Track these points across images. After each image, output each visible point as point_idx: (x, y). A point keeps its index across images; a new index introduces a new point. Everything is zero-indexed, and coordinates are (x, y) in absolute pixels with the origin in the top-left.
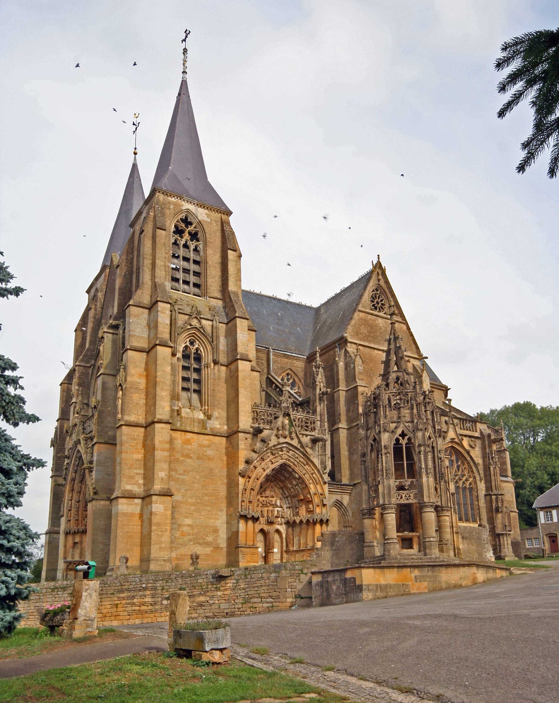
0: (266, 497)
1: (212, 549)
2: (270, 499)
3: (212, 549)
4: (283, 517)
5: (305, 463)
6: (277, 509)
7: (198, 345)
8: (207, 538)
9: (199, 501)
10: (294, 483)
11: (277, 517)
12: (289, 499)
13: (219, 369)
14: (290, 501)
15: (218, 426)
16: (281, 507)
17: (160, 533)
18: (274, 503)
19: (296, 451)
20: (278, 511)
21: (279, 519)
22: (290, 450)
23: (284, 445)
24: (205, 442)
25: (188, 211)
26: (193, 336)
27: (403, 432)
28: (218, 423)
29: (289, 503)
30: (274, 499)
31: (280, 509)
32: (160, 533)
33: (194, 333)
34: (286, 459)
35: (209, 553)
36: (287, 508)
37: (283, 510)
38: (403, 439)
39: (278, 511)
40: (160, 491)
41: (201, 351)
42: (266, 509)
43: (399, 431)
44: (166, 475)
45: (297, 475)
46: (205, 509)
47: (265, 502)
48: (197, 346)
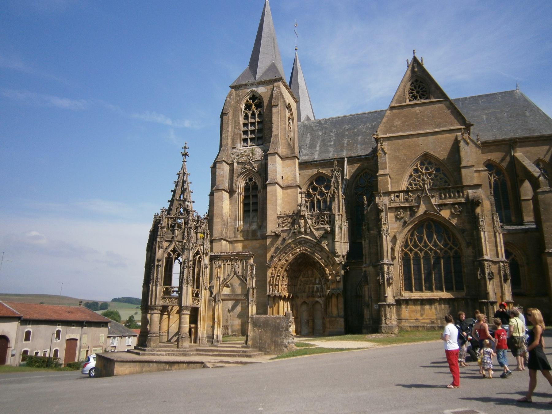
0: (306, 277)
2: (311, 279)
4: (320, 292)
6: (316, 286)
11: (316, 292)
16: (319, 284)
20: (317, 287)
21: (319, 294)
22: (308, 242)
24: (257, 245)
26: (250, 175)
27: (174, 248)
30: (313, 279)
31: (318, 286)
33: (249, 173)
37: (322, 286)
38: (174, 254)
39: (317, 287)
42: (307, 286)
43: (171, 248)
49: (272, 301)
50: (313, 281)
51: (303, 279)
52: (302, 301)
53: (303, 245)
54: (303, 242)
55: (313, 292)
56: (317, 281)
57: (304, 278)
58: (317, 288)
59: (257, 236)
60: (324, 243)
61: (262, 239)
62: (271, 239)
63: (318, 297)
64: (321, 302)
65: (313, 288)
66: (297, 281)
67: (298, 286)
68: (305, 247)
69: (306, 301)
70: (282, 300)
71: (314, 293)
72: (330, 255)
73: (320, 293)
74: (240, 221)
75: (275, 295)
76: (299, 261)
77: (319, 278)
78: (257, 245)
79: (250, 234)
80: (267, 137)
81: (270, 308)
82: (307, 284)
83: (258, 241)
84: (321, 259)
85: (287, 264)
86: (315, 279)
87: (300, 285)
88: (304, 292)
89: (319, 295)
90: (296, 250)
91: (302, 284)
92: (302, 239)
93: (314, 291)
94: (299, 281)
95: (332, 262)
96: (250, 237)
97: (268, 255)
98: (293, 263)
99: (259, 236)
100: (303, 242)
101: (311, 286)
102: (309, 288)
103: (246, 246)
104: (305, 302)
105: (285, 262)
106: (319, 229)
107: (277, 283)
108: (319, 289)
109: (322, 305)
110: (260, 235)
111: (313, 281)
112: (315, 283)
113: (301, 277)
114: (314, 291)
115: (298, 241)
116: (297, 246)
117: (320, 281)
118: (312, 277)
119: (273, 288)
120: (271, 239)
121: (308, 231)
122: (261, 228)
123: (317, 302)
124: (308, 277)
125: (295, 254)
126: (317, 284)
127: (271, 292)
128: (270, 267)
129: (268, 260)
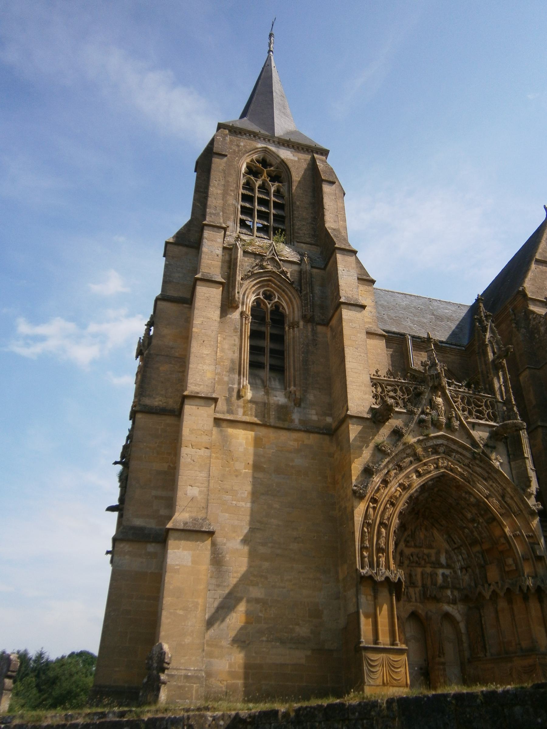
0: (415, 546)
1: (309, 653)
2: (426, 551)
3: (309, 653)
5: (486, 475)
7: (279, 298)
8: (297, 629)
11: (443, 588)
12: (464, 551)
13: (313, 330)
14: (465, 556)
15: (315, 418)
16: (448, 566)
17: (181, 612)
18: (433, 559)
19: (464, 452)
20: (443, 574)
21: (449, 592)
22: (453, 451)
24: (291, 443)
25: (265, 150)
26: (268, 286)
28: (314, 412)
30: (433, 552)
31: (447, 572)
32: (181, 612)
34: (446, 468)
35: (303, 661)
36: (461, 569)
37: (455, 572)
39: (443, 574)
40: (186, 524)
41: (283, 308)
42: (419, 570)
44: (200, 492)
45: (472, 500)
47: (415, 558)
48: (276, 300)
49: (370, 598)
50: (433, 559)
54: (441, 449)
59: (292, 421)
60: (496, 459)
61: (307, 431)
62: (360, 428)
63: (448, 603)
64: (458, 617)
68: (449, 461)
72: (509, 490)
73: (452, 592)
74: (244, 376)
77: (447, 552)
78: (291, 443)
79: (273, 413)
80: (301, 232)
81: (367, 616)
82: (419, 565)
83: (295, 435)
84: (487, 498)
85: (406, 496)
86: (438, 553)
90: (425, 464)
92: (440, 442)
93: (438, 584)
95: (516, 508)
96: (272, 421)
97: (353, 466)
99: (297, 421)
100: (441, 449)
103: (262, 439)
106: (476, 427)
109: (462, 626)
110: (300, 420)
115: (430, 443)
116: (428, 457)
118: (430, 547)
119: (371, 557)
120: (360, 428)
121: (456, 424)
122: (303, 405)
124: (421, 547)
125: (425, 474)
128: (361, 497)
129: (354, 478)
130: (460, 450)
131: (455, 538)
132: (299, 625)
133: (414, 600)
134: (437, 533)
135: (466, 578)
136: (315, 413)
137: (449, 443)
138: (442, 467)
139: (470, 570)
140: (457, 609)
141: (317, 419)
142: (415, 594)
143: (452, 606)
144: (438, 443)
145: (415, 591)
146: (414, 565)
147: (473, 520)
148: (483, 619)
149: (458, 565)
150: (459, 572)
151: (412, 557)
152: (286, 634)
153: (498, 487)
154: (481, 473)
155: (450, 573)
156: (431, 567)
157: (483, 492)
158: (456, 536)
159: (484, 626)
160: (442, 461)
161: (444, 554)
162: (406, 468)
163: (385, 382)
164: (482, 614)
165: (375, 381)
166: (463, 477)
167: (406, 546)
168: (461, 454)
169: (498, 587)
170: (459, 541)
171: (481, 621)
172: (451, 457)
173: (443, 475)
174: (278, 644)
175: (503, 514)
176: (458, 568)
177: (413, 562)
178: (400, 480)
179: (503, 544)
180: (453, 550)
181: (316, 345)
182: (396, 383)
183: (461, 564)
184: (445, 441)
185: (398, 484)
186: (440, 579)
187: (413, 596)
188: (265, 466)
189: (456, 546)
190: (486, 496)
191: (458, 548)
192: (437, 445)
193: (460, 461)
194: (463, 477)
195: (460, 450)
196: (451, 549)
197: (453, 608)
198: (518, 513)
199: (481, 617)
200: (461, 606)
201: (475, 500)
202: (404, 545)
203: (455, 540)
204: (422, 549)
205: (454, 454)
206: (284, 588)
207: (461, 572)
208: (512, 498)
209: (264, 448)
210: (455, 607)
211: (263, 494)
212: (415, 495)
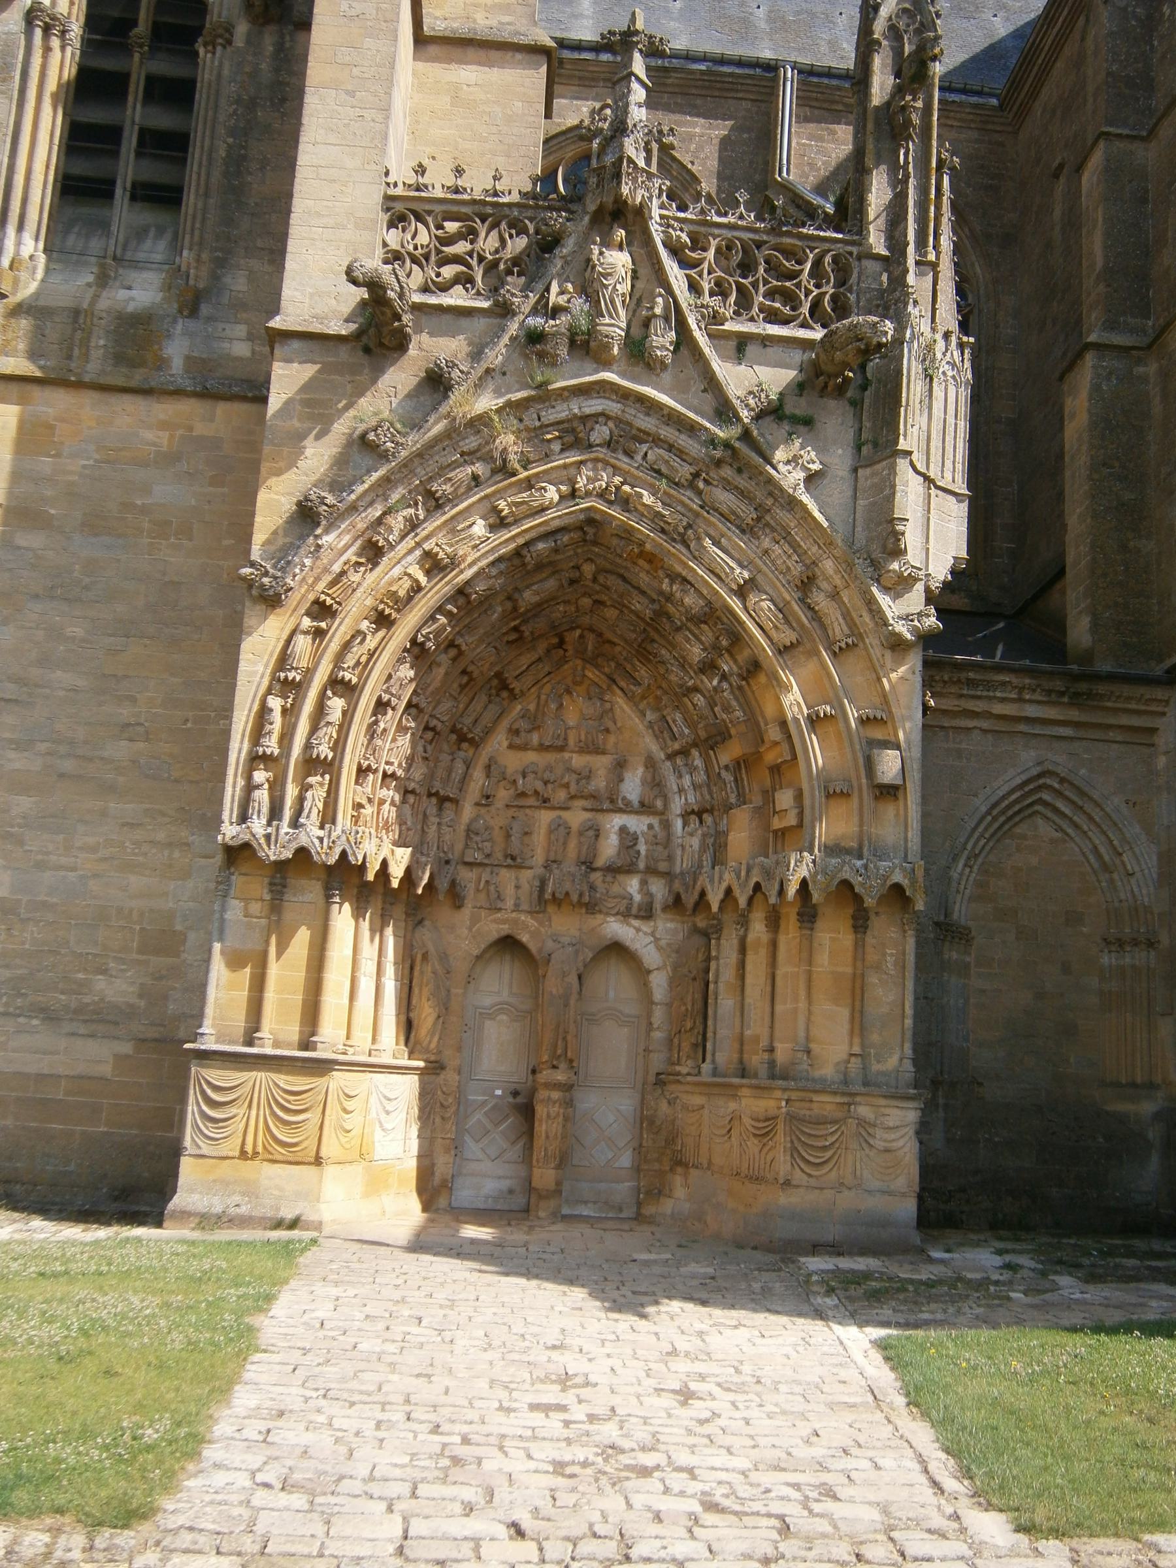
0: (542, 748)
1: (126, 1048)
2: (578, 761)
3: (126, 1048)
4: (651, 871)
6: (617, 821)
8: (100, 983)
9: (68, 765)
10: (696, 653)
11: (613, 870)
12: (698, 762)
13: (280, 48)
14: (701, 777)
16: (645, 808)
18: (599, 783)
19: (683, 441)
20: (623, 830)
21: (633, 885)
22: (642, 436)
23: (593, 406)
24: (149, 435)
29: (695, 787)
30: (601, 764)
31: (637, 824)
34: (602, 495)
35: (106, 1070)
37: (667, 825)
39: (623, 830)
42: (545, 817)
46: (104, 813)
49: (255, 908)
51: (513, 762)
52: (493, 929)
53: (602, 453)
54: (601, 433)
55: (588, 865)
56: (632, 787)
57: (524, 748)
58: (628, 839)
59: (162, 364)
60: (794, 461)
61: (205, 394)
62: (308, 371)
63: (626, 914)
64: (650, 956)
65: (597, 833)
66: (468, 765)
67: (468, 811)
68: (616, 470)
69: (525, 938)
70: (347, 907)
71: (596, 877)
72: (828, 565)
73: (644, 883)
74: (20, 228)
75: (302, 853)
76: (529, 597)
77: (650, 764)
78: (149, 435)
79: (100, 341)
81: (235, 962)
82: (545, 802)
84: (741, 592)
85: (437, 591)
86: (620, 766)
87: (487, 798)
88: (514, 861)
89: (637, 898)
90: (529, 484)
91: (503, 795)
92: (593, 406)
93: (600, 862)
94: (478, 774)
95: (838, 629)
96: (94, 366)
97: (263, 496)
98: (487, 599)
99: (177, 365)
100: (601, 433)
101: (577, 817)
102: (559, 829)
103: (51, 428)
104: (508, 944)
105: (423, 580)
106: (752, 350)
107: (324, 750)
108: (642, 848)
109: (659, 983)
110: (188, 358)
111: (599, 783)
112: (614, 803)
113: (499, 741)
114: (600, 862)
115: (559, 412)
116: (547, 457)
117: (655, 783)
118: (592, 748)
119: (277, 788)
120: (308, 371)
121: (662, 340)
122: (205, 309)
123: (617, 949)
124: (562, 749)
126: (627, 808)
127: (258, 825)
128: (272, 601)
129: (259, 538)
130: (667, 433)
131: (674, 721)
132: (104, 972)
133: (510, 903)
134: (625, 707)
135: (695, 842)
136: (243, 334)
137: (627, 409)
138: (588, 494)
139: (708, 819)
140: (653, 934)
141: (248, 354)
142: (517, 887)
143: (636, 923)
144: (587, 411)
145: (517, 879)
146: (531, 801)
147: (708, 667)
148: (713, 965)
149: (677, 805)
150: (679, 823)
151: (524, 777)
152: (63, 997)
153: (789, 556)
154: (734, 513)
155: (650, 827)
156: (585, 810)
157: (726, 573)
158: (678, 716)
159: (711, 986)
160: (591, 473)
161: (640, 771)
162: (452, 500)
163: (438, 208)
164: (714, 954)
165: (399, 207)
166: (662, 524)
167: (511, 747)
168: (670, 448)
169: (739, 877)
170: (687, 731)
171: (707, 971)
172: (632, 458)
173: (591, 523)
174: (35, 1022)
175: (785, 647)
176: (678, 812)
177: (523, 795)
178: (427, 538)
179: (776, 743)
180: (670, 757)
181: (284, 100)
182: (477, 208)
183: (686, 799)
184: (615, 405)
185: (418, 553)
186: (610, 847)
187: (509, 892)
188: (52, 512)
189: (677, 746)
190: (735, 587)
191: (684, 752)
192: (584, 419)
193: (664, 470)
194: (662, 524)
195: (667, 433)
196: (663, 756)
197: (638, 930)
198: (843, 645)
199: (708, 959)
200: (667, 926)
201: (702, 602)
202: (505, 744)
203: (675, 729)
204: (566, 755)
205: (644, 447)
206: (73, 869)
207: (685, 824)
208: (835, 596)
209: (58, 455)
210: (646, 927)
211: (37, 596)
212: (480, 587)
